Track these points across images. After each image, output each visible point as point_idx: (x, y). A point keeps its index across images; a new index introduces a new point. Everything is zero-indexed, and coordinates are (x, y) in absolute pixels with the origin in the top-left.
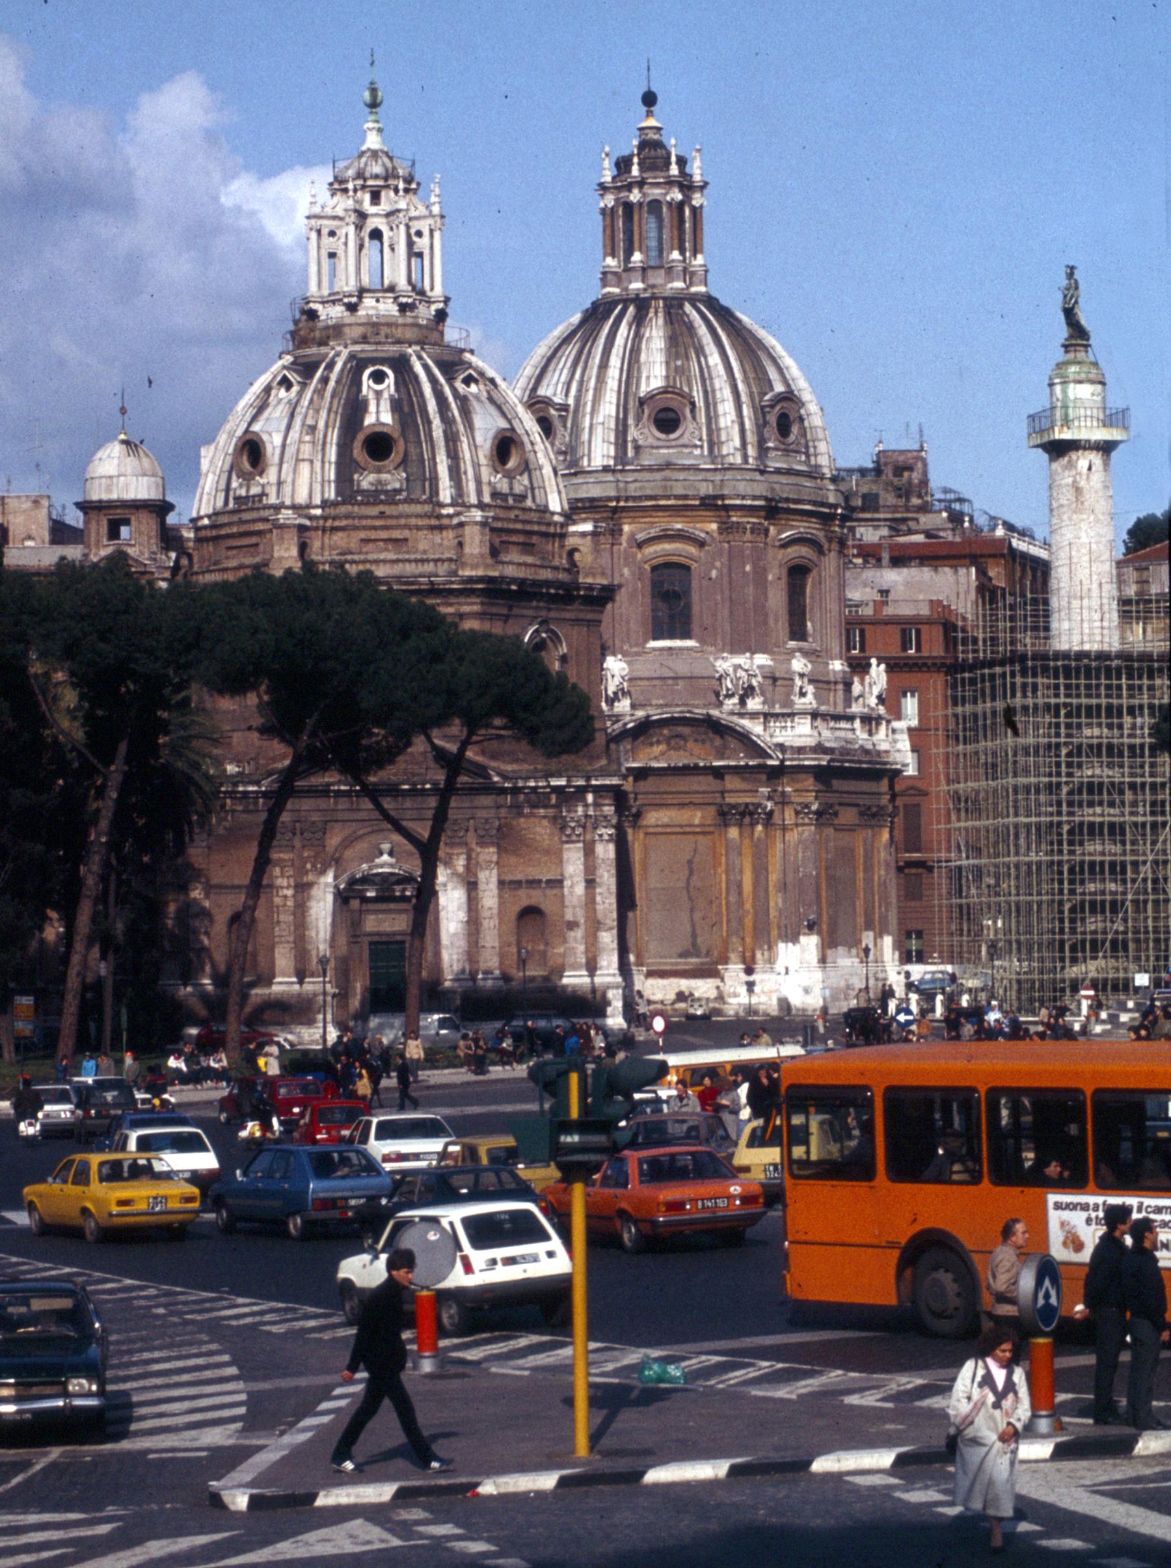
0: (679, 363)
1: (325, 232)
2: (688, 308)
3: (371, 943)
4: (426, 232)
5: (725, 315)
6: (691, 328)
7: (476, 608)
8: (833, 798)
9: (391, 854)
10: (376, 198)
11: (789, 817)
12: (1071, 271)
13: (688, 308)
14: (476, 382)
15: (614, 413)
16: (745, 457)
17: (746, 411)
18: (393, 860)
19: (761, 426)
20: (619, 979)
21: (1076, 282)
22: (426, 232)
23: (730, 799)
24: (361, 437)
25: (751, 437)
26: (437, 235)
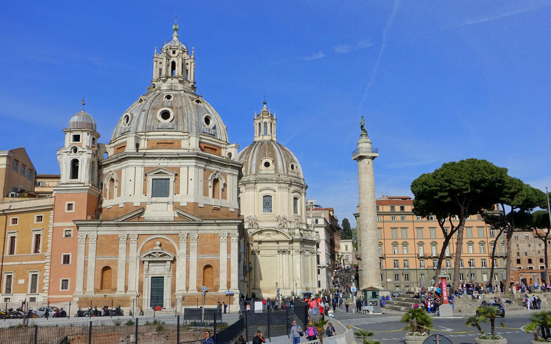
1: (159, 62)
3: (152, 277)
4: (189, 63)
5: (280, 145)
6: (273, 147)
7: (194, 164)
8: (304, 249)
9: (160, 246)
10: (174, 52)
11: (294, 253)
13: (272, 143)
18: (160, 248)
19: (287, 167)
20: (238, 291)
22: (189, 63)
23: (281, 248)
25: (285, 168)
26: (192, 64)
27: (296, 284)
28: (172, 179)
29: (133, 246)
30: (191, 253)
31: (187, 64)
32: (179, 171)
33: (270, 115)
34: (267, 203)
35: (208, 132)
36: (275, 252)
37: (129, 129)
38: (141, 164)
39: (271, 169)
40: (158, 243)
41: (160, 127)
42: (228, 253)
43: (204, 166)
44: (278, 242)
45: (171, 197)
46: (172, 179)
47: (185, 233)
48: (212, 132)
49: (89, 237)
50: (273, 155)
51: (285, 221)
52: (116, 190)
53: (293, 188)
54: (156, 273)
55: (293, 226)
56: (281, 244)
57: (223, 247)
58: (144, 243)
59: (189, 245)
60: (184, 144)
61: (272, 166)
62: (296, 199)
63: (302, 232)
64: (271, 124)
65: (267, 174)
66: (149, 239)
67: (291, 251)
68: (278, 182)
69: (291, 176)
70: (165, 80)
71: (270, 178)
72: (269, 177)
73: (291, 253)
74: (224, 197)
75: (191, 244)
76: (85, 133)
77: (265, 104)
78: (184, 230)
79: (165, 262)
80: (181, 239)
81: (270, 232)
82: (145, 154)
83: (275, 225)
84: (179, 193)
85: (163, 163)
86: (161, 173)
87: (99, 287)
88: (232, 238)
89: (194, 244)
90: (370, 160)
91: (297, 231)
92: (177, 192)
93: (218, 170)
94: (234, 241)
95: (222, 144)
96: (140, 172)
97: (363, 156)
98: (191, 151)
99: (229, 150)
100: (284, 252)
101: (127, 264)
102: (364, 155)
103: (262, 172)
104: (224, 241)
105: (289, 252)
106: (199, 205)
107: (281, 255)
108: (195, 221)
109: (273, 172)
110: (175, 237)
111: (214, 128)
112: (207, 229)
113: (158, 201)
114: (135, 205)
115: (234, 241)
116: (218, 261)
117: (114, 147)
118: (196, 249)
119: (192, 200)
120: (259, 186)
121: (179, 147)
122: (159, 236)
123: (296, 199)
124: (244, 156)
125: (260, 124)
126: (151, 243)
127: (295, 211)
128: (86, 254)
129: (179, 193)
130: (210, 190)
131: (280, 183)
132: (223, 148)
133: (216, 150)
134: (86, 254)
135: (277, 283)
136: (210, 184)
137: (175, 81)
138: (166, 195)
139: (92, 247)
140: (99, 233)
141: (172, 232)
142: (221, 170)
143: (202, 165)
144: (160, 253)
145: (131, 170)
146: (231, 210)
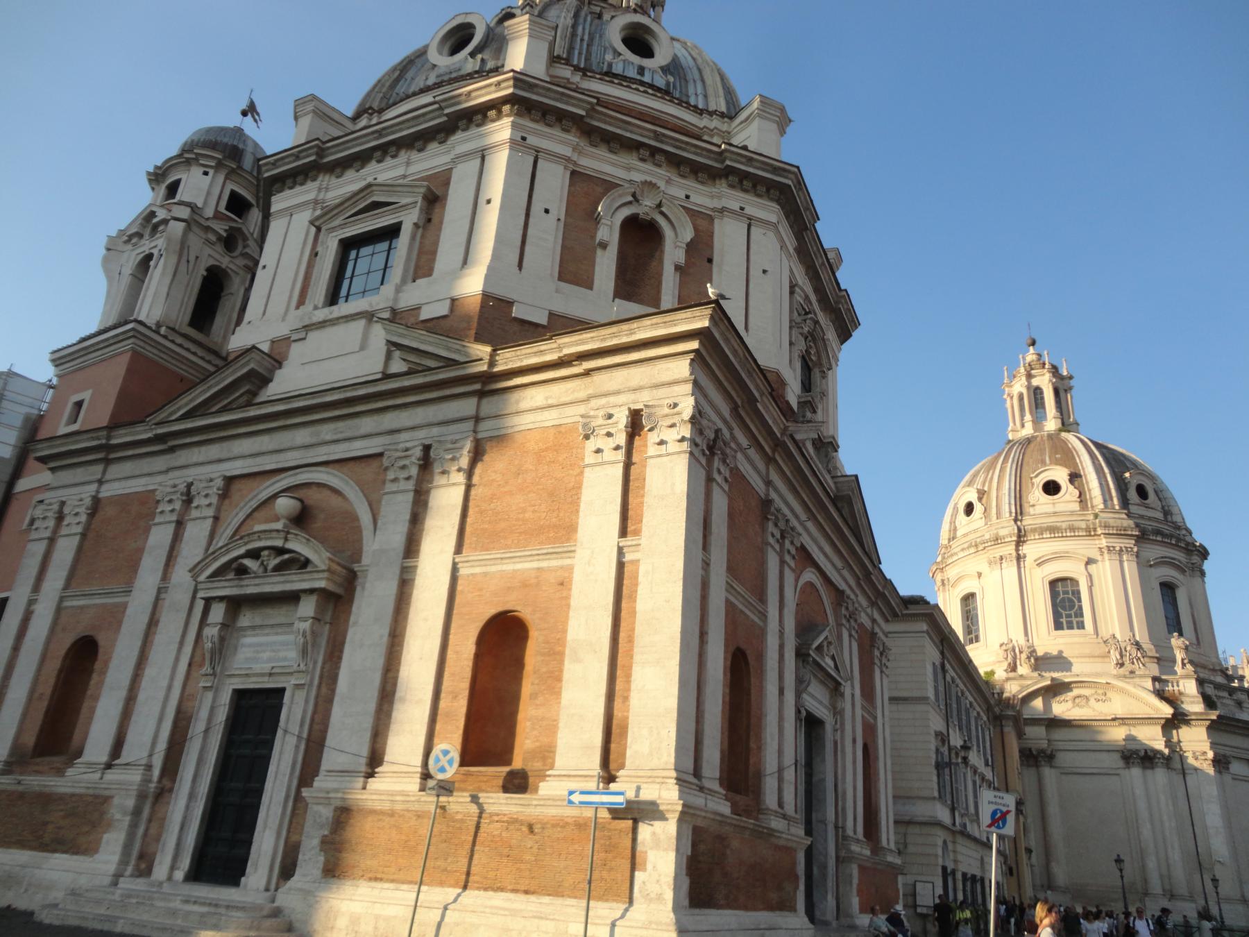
27: (1215, 880)
29: (197, 532)
39: (1067, 497)
42: (623, 533)
43: (567, 151)
47: (413, 442)
49: (66, 510)
50: (1066, 457)
54: (257, 668)
58: (241, 516)
61: (1068, 492)
62: (1168, 589)
71: (1064, 525)
76: (196, 172)
77: (1033, 343)
79: (292, 598)
87: (30, 739)
101: (153, 623)
103: (1038, 509)
107: (1136, 772)
109: (1076, 507)
110: (368, 471)
116: (564, 584)
124: (980, 479)
128: (37, 588)
130: (606, 266)
134: (37, 588)
135: (1119, 861)
139: (66, 550)
140: (107, 491)
143: (558, 142)
144: (280, 551)
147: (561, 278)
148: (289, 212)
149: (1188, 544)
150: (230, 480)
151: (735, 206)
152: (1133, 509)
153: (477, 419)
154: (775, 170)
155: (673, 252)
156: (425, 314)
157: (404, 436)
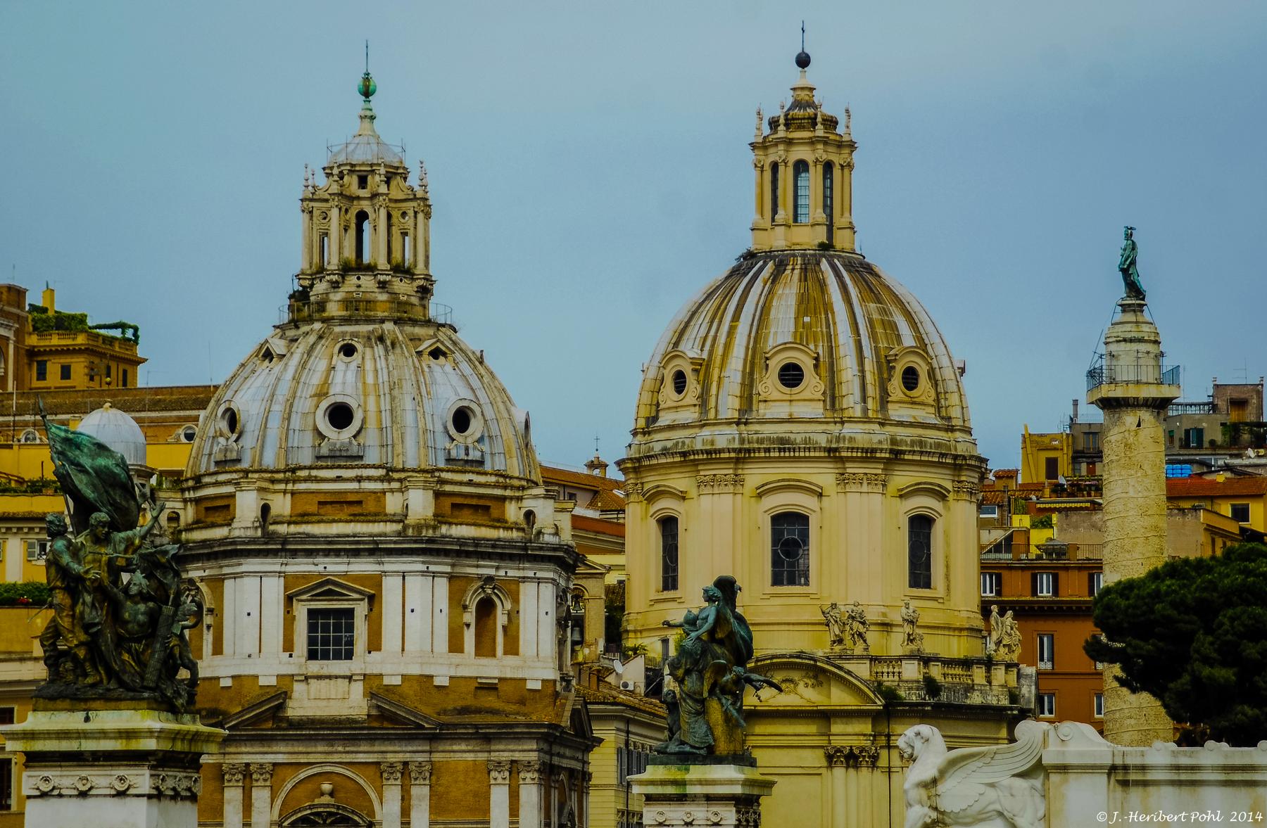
0: (807, 319)
1: (316, 213)
2: (824, 264)
6: (822, 285)
9: (331, 794)
10: (363, 182)
12: (1129, 236)
13: (824, 264)
14: (444, 354)
15: (741, 368)
16: (865, 410)
17: (869, 366)
18: (332, 801)
21: (1133, 243)
22: (411, 213)
23: (837, 742)
24: (325, 404)
28: (361, 609)
29: (261, 796)
30: (413, 814)
31: (404, 214)
32: (379, 586)
33: (820, 131)
34: (790, 545)
35: (463, 456)
36: (815, 759)
37: (238, 452)
38: (278, 568)
39: (807, 394)
40: (327, 787)
41: (324, 451)
42: (511, 815)
43: (448, 569)
44: (825, 716)
45: (362, 662)
46: (361, 609)
48: (474, 455)
51: (856, 625)
52: (208, 638)
53: (903, 478)
55: (896, 644)
56: (837, 728)
57: (499, 797)
58: (289, 786)
59: (409, 792)
60: (393, 504)
61: (812, 384)
63: (936, 671)
64: (828, 167)
65: (791, 420)
66: (302, 776)
67: (884, 753)
68: (832, 454)
69: (900, 424)
70: (337, 282)
71: (799, 438)
72: (797, 433)
73: (883, 762)
74: (512, 648)
75: (415, 791)
78: (396, 754)
80: (385, 775)
81: (795, 675)
82: (285, 540)
83: (820, 646)
84: (380, 650)
85: (334, 567)
86: (329, 592)
88: (522, 775)
89: (420, 792)
90: (1146, 415)
91: (911, 671)
92: (375, 644)
93: (492, 572)
94: (528, 781)
95: (505, 488)
96: (275, 589)
97: (1117, 399)
98: (410, 532)
99: (528, 504)
100: (852, 759)
102: (1119, 393)
104: (500, 781)
105: (875, 758)
106: (437, 682)
107: (839, 772)
108: (423, 727)
109: (817, 410)
111: (480, 440)
112: (455, 748)
113: (325, 672)
114: (263, 681)
115: (528, 781)
117: (197, 501)
118: (425, 805)
119: (415, 670)
120: (756, 475)
121: (376, 515)
122: (328, 769)
123: (921, 526)
125: (775, 167)
126: (310, 786)
127: (920, 574)
129: (380, 650)
130: (469, 637)
131: (842, 460)
132: (511, 498)
133: (487, 508)
136: (470, 617)
137: (368, 282)
138: (349, 655)
141: (361, 758)
142: (502, 573)
144: (330, 814)
145: (251, 583)
146: (530, 685)
147: (450, 651)
148: (262, 575)
149: (956, 457)
150: (274, 764)
151: (531, 574)
152: (896, 412)
153: (431, 752)
154: (555, 549)
155: (501, 619)
156: (386, 681)
157: (389, 755)
